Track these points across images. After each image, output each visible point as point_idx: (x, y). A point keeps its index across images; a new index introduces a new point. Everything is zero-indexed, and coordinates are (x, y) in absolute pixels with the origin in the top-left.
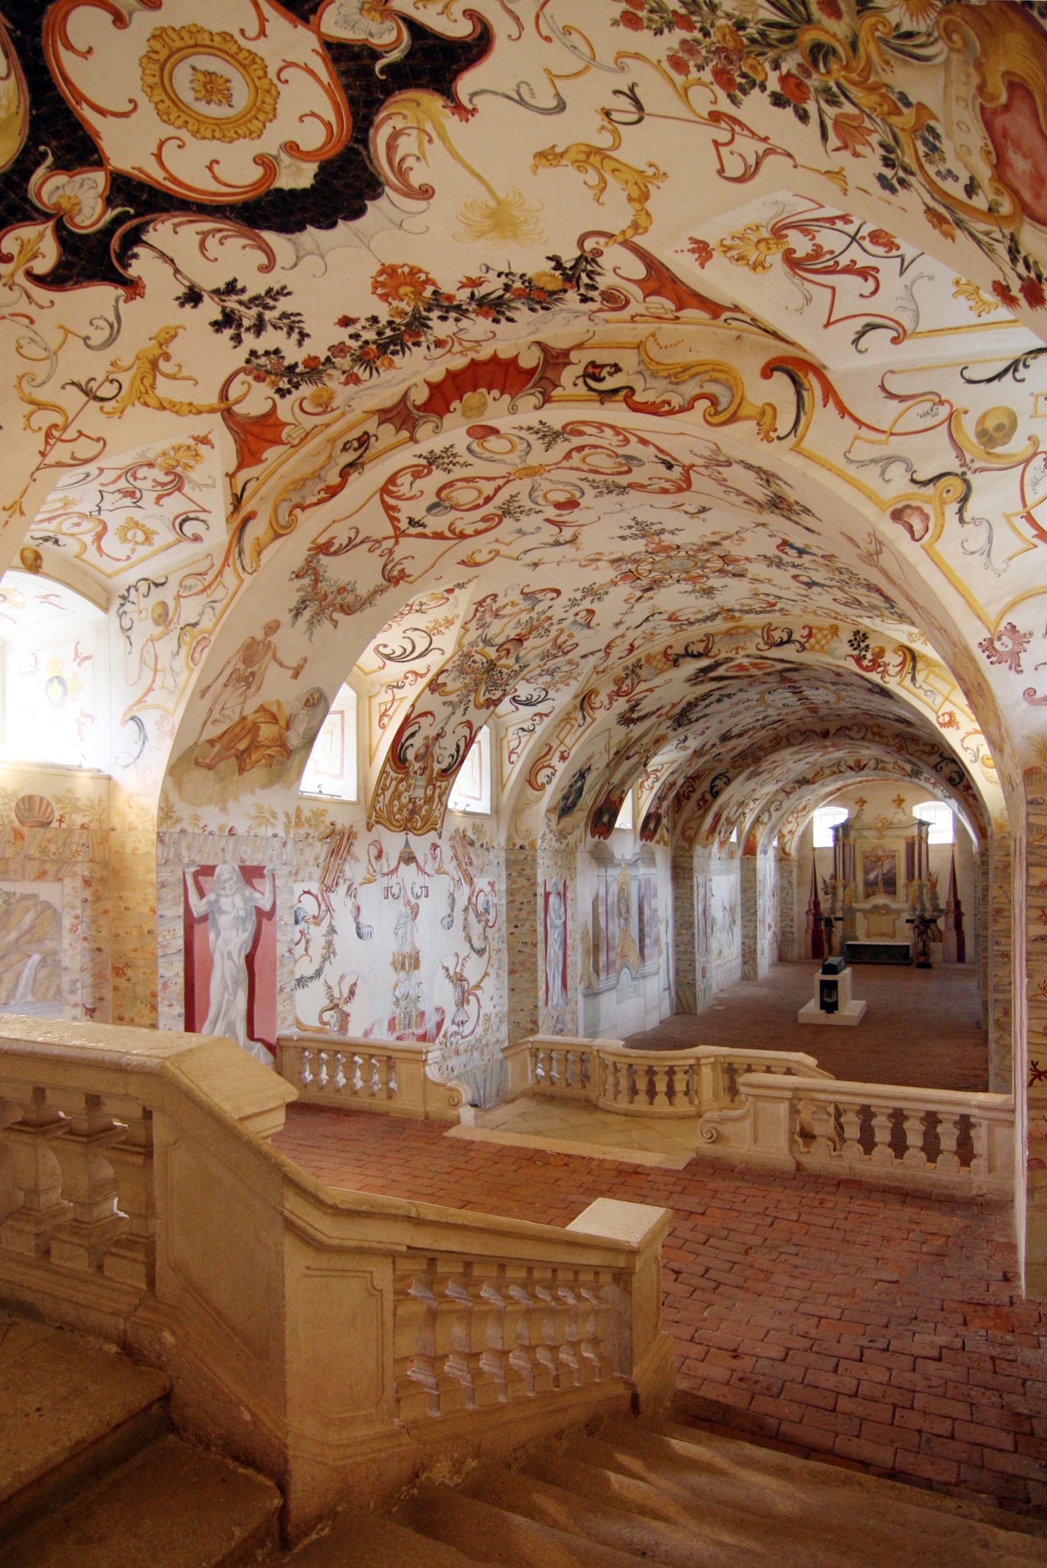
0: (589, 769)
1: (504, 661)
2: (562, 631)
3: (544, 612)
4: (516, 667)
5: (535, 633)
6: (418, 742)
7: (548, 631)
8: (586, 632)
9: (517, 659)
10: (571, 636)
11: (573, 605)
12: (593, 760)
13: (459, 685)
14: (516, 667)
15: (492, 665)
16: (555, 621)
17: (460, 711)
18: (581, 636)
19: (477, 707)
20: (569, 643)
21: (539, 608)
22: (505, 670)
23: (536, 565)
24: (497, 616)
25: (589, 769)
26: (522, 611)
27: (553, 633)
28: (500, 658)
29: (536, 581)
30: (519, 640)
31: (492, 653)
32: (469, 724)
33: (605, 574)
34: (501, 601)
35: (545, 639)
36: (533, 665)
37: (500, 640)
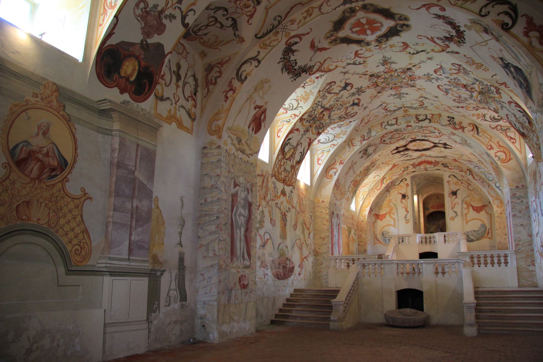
0: (501, 59)
1: (477, 88)
2: (451, 74)
3: (448, 85)
4: (477, 83)
5: (459, 82)
6: (518, 125)
7: (455, 79)
8: (444, 66)
9: (474, 84)
10: (451, 69)
11: (438, 79)
12: (496, 56)
13: (493, 104)
14: (477, 83)
15: (480, 93)
16: (449, 79)
17: (504, 105)
18: (447, 66)
19: (501, 98)
20: (454, 68)
21: (449, 87)
22: (481, 87)
23: (436, 97)
24: (460, 97)
25: (501, 59)
26: (453, 91)
27: (455, 76)
28: (476, 91)
29: (440, 94)
30: (465, 86)
31: (475, 94)
32: (510, 103)
33: (419, 83)
34: (455, 98)
35: (459, 77)
36: (473, 76)
37: (469, 93)
